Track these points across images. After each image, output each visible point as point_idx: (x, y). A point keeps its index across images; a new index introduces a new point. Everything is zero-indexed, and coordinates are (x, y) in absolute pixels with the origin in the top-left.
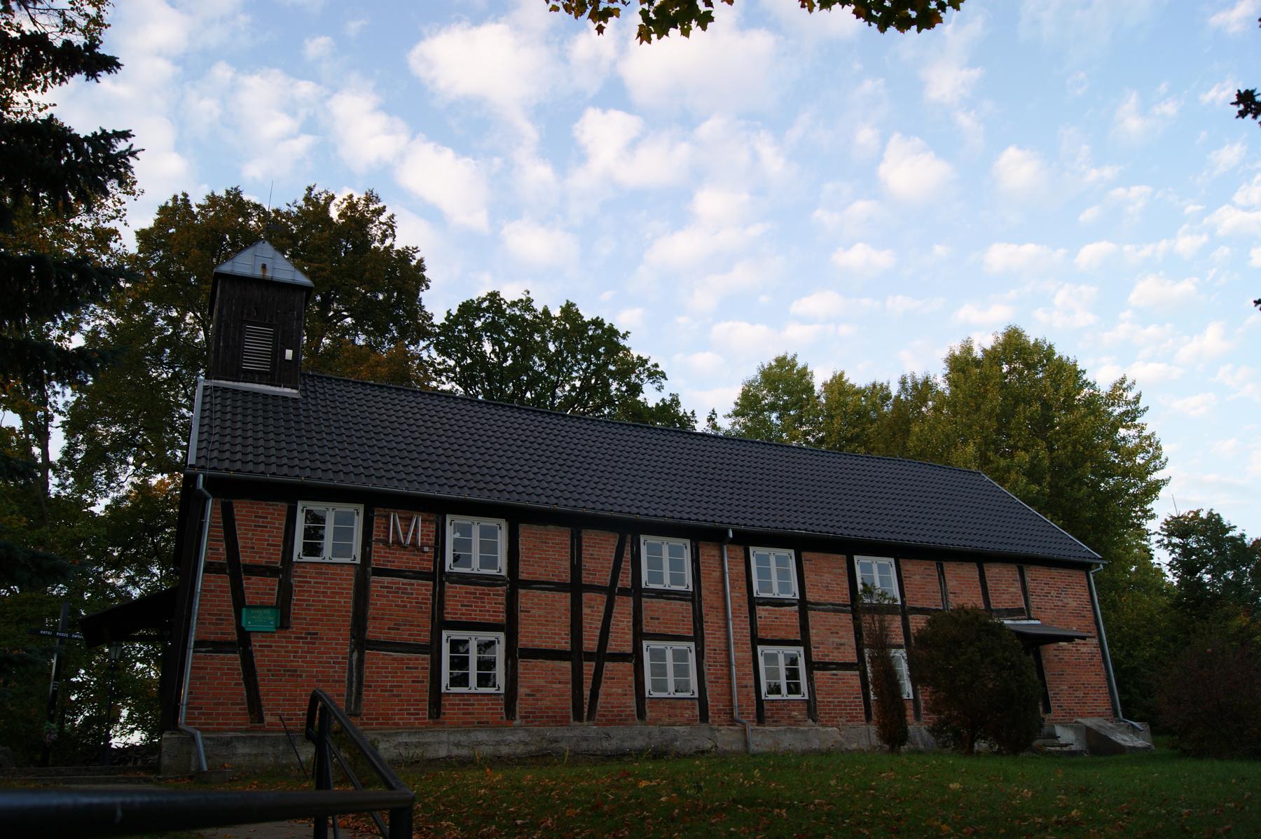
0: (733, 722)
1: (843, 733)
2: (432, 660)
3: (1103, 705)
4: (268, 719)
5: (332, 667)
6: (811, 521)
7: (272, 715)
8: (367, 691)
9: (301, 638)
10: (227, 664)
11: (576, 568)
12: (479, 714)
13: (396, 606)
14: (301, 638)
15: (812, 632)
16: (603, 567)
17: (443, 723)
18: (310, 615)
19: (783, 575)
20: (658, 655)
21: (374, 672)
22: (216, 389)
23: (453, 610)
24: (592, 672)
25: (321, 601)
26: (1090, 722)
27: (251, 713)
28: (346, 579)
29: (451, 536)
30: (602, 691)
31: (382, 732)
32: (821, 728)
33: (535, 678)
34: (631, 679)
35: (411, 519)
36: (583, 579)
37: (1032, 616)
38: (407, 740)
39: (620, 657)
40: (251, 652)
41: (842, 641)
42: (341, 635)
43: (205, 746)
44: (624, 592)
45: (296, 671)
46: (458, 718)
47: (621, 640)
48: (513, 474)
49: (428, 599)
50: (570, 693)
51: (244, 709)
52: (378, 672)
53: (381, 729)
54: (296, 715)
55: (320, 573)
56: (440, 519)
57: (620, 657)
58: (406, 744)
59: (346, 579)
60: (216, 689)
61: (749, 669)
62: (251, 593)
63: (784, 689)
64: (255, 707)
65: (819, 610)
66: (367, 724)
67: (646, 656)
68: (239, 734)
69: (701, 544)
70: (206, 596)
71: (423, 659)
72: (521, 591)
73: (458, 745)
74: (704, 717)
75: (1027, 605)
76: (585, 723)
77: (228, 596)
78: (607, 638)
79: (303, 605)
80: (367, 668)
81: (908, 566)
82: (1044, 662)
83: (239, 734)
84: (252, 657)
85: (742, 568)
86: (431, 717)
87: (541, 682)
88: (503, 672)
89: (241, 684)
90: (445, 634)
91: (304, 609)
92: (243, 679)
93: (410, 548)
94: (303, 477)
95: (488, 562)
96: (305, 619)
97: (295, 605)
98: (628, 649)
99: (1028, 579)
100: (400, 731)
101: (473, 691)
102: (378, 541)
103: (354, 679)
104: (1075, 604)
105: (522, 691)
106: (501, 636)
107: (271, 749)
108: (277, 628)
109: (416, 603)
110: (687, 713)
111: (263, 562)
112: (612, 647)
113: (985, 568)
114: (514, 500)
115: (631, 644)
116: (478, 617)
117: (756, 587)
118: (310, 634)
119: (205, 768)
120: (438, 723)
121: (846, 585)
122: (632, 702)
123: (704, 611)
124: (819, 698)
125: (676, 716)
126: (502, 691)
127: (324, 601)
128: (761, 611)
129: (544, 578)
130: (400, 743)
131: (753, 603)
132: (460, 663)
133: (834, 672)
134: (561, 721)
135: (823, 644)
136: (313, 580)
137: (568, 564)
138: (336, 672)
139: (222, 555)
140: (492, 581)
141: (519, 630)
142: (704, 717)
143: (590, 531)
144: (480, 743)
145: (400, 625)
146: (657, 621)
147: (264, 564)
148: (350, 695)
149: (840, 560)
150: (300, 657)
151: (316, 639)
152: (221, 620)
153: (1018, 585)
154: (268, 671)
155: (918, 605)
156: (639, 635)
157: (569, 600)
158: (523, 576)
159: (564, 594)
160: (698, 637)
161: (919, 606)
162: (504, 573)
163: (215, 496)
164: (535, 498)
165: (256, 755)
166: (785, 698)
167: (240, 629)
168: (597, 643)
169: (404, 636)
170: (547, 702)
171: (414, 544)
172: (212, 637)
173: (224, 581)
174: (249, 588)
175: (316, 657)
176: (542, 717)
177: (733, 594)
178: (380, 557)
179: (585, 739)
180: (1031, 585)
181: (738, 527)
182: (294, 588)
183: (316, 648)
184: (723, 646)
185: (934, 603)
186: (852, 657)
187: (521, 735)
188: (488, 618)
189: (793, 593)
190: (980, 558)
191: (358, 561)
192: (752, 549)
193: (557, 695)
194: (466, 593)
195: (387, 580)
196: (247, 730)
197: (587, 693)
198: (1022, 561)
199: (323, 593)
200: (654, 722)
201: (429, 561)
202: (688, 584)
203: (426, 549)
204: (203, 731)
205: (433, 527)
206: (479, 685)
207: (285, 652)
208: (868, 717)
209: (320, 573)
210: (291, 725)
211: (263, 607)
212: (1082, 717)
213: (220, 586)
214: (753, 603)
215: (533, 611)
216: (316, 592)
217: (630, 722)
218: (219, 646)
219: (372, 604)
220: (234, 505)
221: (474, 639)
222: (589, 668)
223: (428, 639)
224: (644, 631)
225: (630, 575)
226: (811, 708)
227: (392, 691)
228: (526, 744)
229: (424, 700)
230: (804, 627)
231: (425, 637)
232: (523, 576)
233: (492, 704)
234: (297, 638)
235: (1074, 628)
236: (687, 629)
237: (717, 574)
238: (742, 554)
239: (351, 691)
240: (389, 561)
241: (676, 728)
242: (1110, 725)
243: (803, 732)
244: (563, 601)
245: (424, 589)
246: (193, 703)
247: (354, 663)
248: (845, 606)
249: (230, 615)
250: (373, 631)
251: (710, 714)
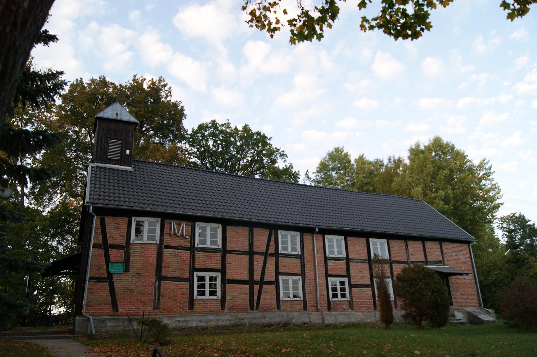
0: (317, 310)
1: (364, 315)
2: (190, 284)
3: (475, 302)
4: (120, 310)
5: (147, 288)
6: (351, 224)
7: (122, 309)
8: (162, 298)
9: (134, 276)
10: (103, 287)
11: (251, 245)
12: (209, 307)
13: (175, 261)
14: (134, 276)
15: (351, 271)
16: (262, 244)
17: (194, 312)
18: (138, 266)
19: (339, 247)
20: (286, 282)
21: (165, 290)
22: (97, 167)
23: (199, 263)
24: (258, 289)
25: (142, 260)
26: (469, 309)
27: (113, 308)
28: (153, 250)
29: (198, 231)
30: (262, 298)
31: (169, 316)
32: (355, 313)
33: (233, 292)
34: (274, 292)
35: (180, 224)
36: (254, 250)
37: (445, 264)
38: (180, 319)
39: (270, 283)
40: (113, 282)
41: (364, 275)
42: (151, 274)
43: (94, 322)
44: (271, 255)
45: (132, 290)
46: (201, 310)
47: (270, 276)
48: (224, 204)
49: (188, 259)
50: (248, 298)
51: (110, 306)
52: (167, 290)
53: (168, 314)
54: (132, 309)
55: (142, 248)
56: (193, 224)
57: (270, 283)
58: (179, 321)
59: (153, 250)
60: (98, 298)
61: (325, 287)
62: (113, 257)
63: (339, 296)
64: (115, 305)
65: (354, 262)
66: (163, 312)
67: (281, 282)
68: (108, 317)
69: (304, 234)
70: (94, 258)
71: (186, 284)
72: (228, 255)
73: (201, 321)
74: (305, 308)
75: (443, 259)
76: (255, 311)
77: (103, 258)
78: (264, 275)
79: (134, 262)
80: (162, 288)
81: (392, 242)
82: (450, 283)
83: (108, 317)
84: (113, 284)
85: (322, 244)
86: (189, 309)
87: (237, 294)
88: (220, 290)
89: (108, 296)
90: (195, 273)
91: (136, 263)
92: (110, 293)
93: (180, 237)
94: (134, 206)
95: (213, 242)
96: (136, 268)
97: (132, 261)
98: (273, 279)
99: (443, 248)
100: (176, 315)
101: (207, 298)
102: (167, 234)
103: (157, 293)
104: (463, 258)
105: (228, 298)
106: (219, 274)
107: (122, 323)
108: (124, 271)
109: (183, 260)
110: (298, 307)
111: (118, 243)
112: (266, 279)
113: (425, 244)
114: (224, 216)
115: (274, 277)
116: (209, 266)
117: (327, 252)
118: (137, 274)
119: (94, 333)
120: (192, 312)
121: (366, 251)
122: (275, 302)
123: (305, 263)
124: (354, 300)
125: (293, 308)
126: (220, 298)
127: (144, 260)
128: (330, 263)
129: (237, 249)
130: (176, 321)
131: (326, 259)
132: (202, 286)
133: (361, 288)
134: (245, 310)
135: (356, 276)
136: (139, 251)
137: (247, 243)
138: (149, 290)
139: (100, 241)
140: (215, 251)
141: (227, 272)
142: (305, 308)
143: (257, 229)
144: (210, 321)
145: (176, 270)
146: (285, 267)
147: (118, 244)
148: (155, 300)
149: (363, 240)
150: (134, 284)
151: (140, 276)
152: (100, 268)
153: (439, 250)
154: (120, 290)
155: (397, 259)
156: (278, 273)
157: (248, 259)
158: (228, 248)
159: (246, 256)
160: (303, 274)
161: (397, 260)
162: (220, 247)
163: (97, 215)
164: (234, 215)
165: (115, 326)
166: (340, 300)
167: (108, 272)
168: (260, 277)
169: (178, 274)
170: (239, 302)
171: (182, 235)
172: (96, 276)
173: (101, 251)
174: (112, 255)
175: (141, 284)
176: (236, 309)
177: (318, 256)
178: (168, 240)
179: (255, 318)
180: (445, 251)
181: (319, 227)
182: (131, 254)
183: (140, 280)
184: (313, 278)
185: (403, 258)
186: (368, 282)
187: (228, 317)
188: (213, 267)
189: (343, 255)
190: (423, 239)
191: (158, 243)
192: (326, 236)
193: (243, 299)
194: (204, 256)
195: (170, 250)
196: (111, 315)
197: (255, 298)
198: (441, 240)
199: (144, 256)
200: (284, 311)
201: (188, 242)
202: (298, 252)
203: (187, 237)
204: (92, 316)
205: (190, 228)
206: (210, 295)
207: (128, 282)
208: (375, 308)
209: (142, 248)
210: (130, 313)
211: (118, 262)
212: (466, 307)
213: (100, 254)
214: (326, 259)
215: (233, 264)
216: (140, 256)
217: (274, 311)
218: (99, 280)
219: (164, 261)
220: (105, 219)
221: (207, 275)
222: (256, 287)
223: (188, 276)
224: (280, 271)
225: (274, 248)
226: (351, 304)
227: (173, 298)
228: (230, 321)
229: (187, 302)
230: (348, 269)
231: (187, 275)
232: (228, 248)
233: (216, 303)
234: (132, 276)
235: (463, 269)
236: (298, 270)
237: (311, 247)
238: (322, 238)
239: (156, 298)
240: (171, 243)
241: (293, 313)
242: (478, 310)
243: (347, 315)
245: (186, 254)
246: (88, 304)
247: (157, 286)
248: (366, 260)
249: (104, 266)
250: (165, 272)
251: (308, 307)
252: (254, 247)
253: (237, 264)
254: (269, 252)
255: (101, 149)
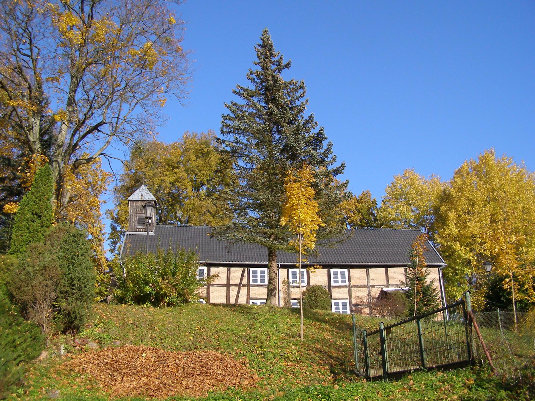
11: (228, 280)
44: (244, 286)
244: (225, 288)
252: (231, 281)
253: (217, 293)
254: (242, 284)
255: (133, 222)
